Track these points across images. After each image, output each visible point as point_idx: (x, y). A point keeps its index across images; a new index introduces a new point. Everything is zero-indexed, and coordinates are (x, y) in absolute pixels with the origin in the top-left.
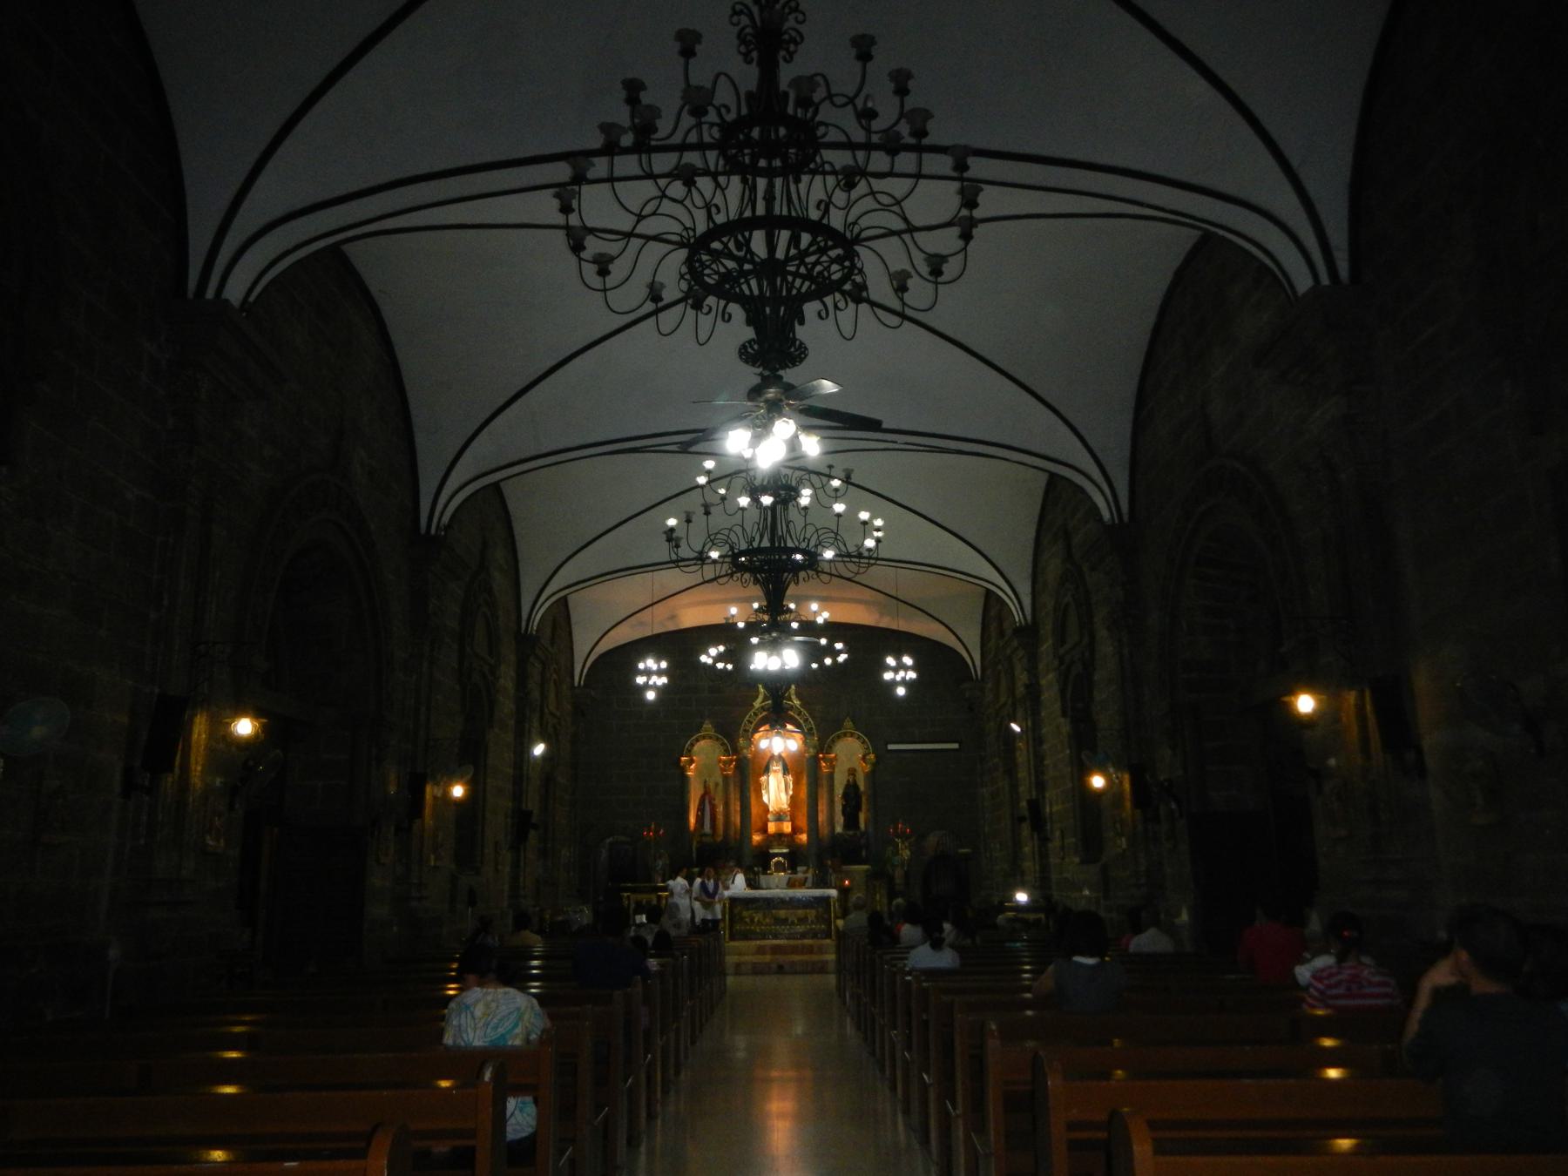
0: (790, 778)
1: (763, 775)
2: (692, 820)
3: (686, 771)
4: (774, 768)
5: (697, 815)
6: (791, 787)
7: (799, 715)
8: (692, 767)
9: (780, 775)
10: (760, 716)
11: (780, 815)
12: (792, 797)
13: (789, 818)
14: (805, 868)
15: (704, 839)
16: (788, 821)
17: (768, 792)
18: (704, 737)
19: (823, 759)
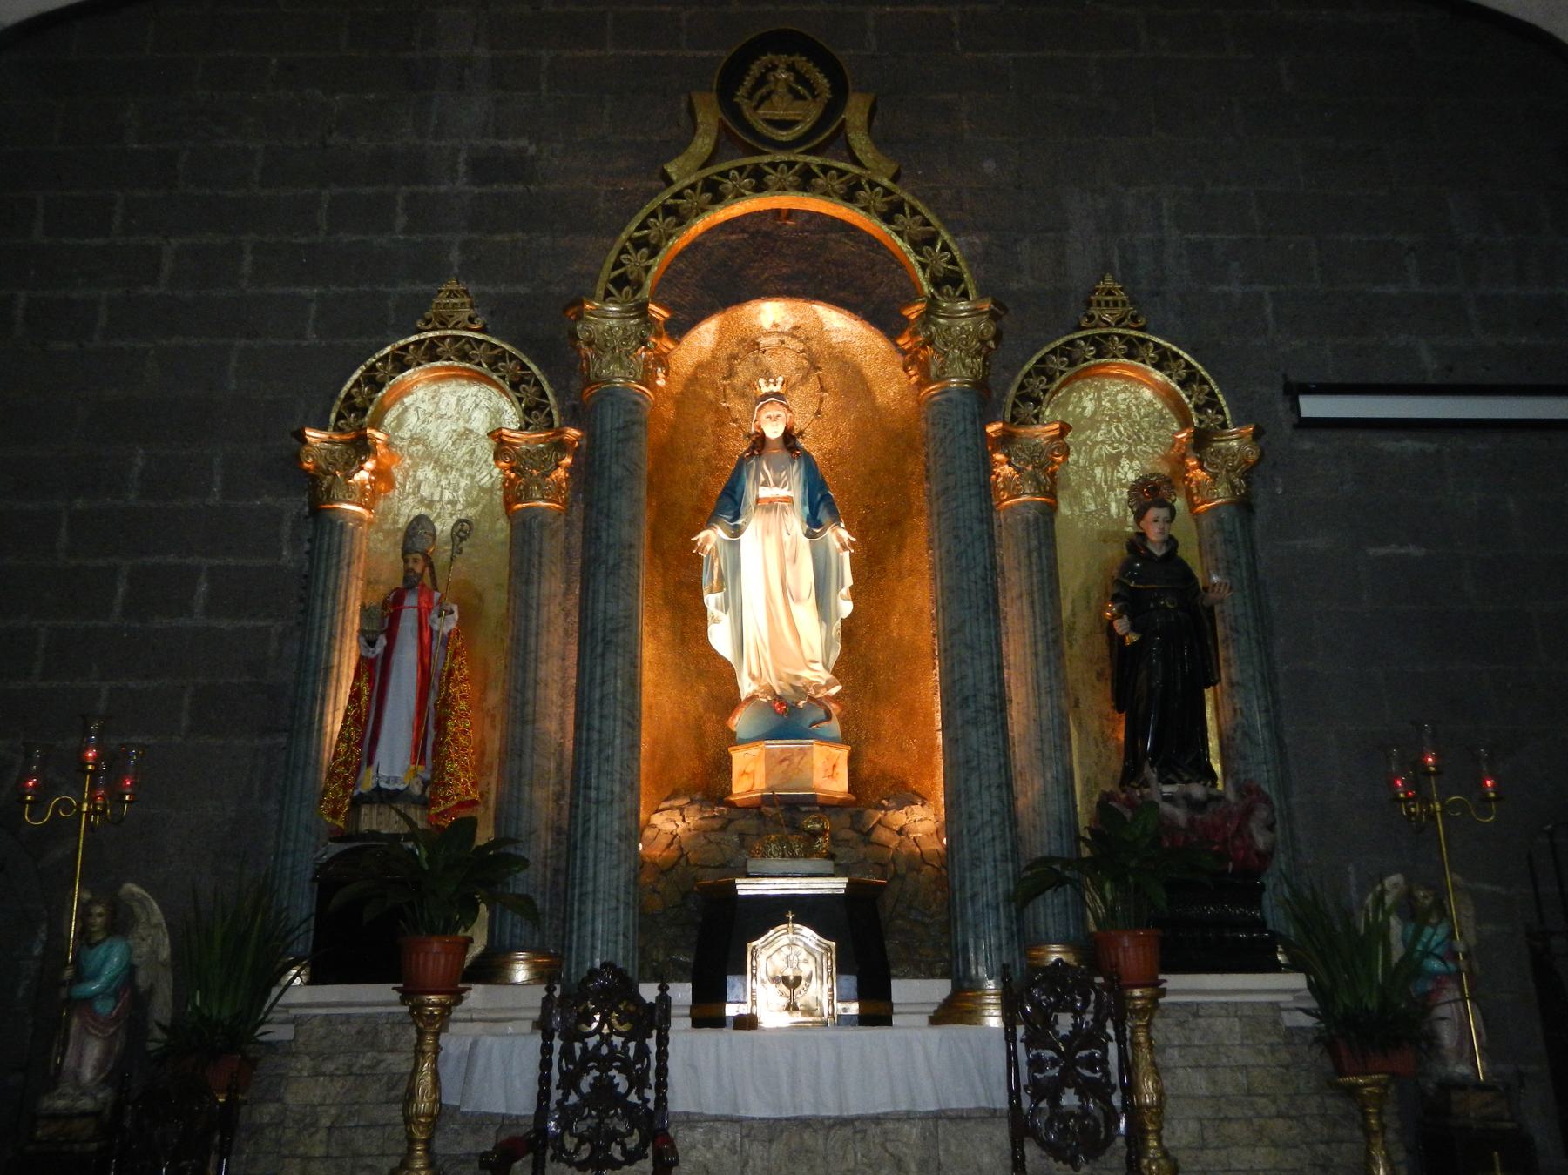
0: (837, 536)
1: (708, 524)
2: (334, 722)
3: (331, 500)
4: (764, 492)
5: (355, 696)
6: (849, 580)
7: (887, 218)
8: (362, 476)
9: (795, 524)
10: (699, 226)
11: (792, 709)
12: (849, 631)
13: (834, 727)
14: (940, 989)
15: (370, 820)
16: (833, 741)
17: (734, 606)
18: (431, 352)
19: (1006, 440)
